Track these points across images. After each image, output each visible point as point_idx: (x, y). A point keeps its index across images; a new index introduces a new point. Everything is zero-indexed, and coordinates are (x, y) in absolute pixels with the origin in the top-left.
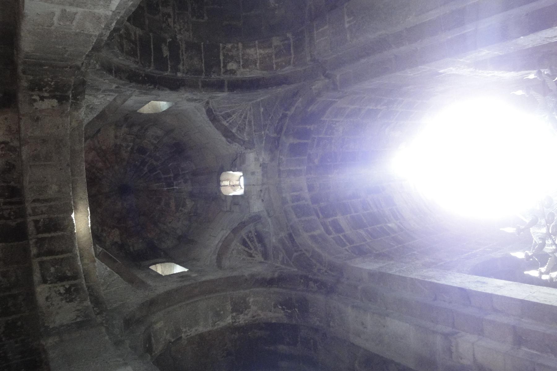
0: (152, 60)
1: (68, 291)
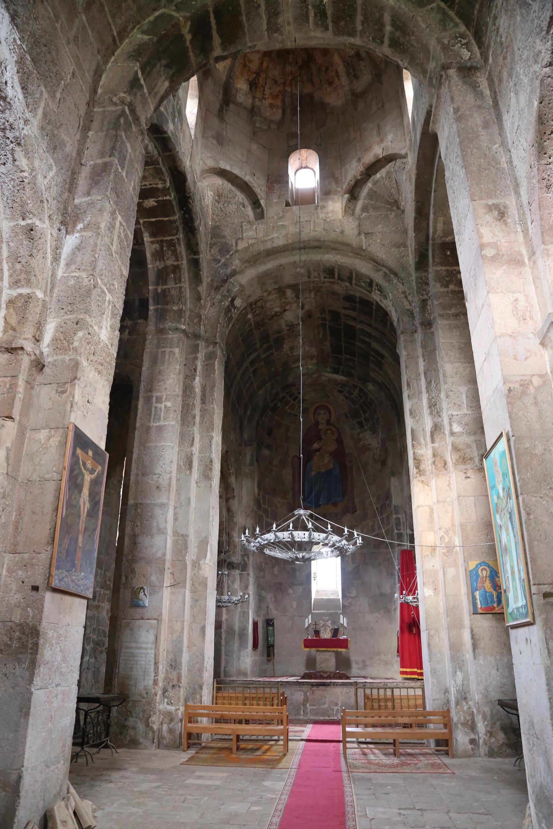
0: (167, 219)
1: (379, 291)
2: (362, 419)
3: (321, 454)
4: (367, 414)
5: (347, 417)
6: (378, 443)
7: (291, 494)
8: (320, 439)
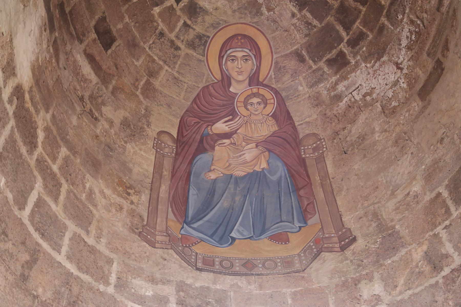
2: (343, 47)
3: (231, 143)
4: (357, 25)
5: (302, 59)
6: (398, 66)
7: (145, 198)
8: (233, 114)
